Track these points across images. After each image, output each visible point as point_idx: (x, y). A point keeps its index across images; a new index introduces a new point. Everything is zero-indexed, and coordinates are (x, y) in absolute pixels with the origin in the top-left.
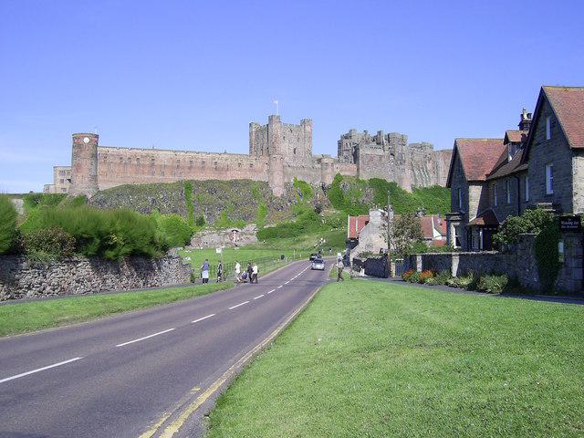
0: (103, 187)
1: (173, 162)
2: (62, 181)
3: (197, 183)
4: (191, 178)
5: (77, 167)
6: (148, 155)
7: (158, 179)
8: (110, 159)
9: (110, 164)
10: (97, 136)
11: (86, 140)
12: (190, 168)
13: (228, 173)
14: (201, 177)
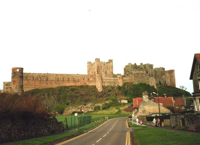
0: (26, 89)
2: (7, 88)
4: (63, 85)
5: (14, 82)
7: (49, 86)
10: (22, 69)
11: (18, 70)
14: (67, 84)
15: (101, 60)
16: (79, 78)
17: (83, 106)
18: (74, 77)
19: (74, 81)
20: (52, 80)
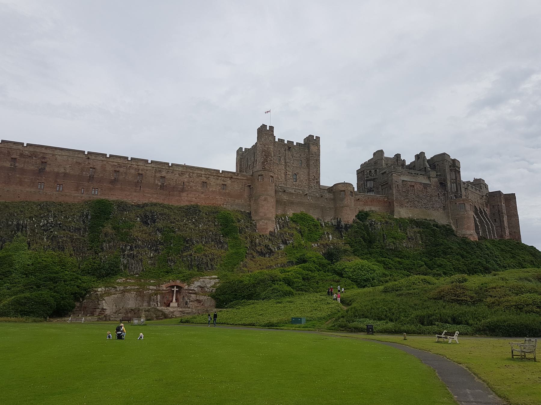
3: (123, 206)
6: (33, 155)
12: (114, 182)
13: (184, 194)
14: (133, 197)
15: (278, 135)
17: (178, 283)
18: (164, 174)
19: (162, 187)
20: (66, 175)
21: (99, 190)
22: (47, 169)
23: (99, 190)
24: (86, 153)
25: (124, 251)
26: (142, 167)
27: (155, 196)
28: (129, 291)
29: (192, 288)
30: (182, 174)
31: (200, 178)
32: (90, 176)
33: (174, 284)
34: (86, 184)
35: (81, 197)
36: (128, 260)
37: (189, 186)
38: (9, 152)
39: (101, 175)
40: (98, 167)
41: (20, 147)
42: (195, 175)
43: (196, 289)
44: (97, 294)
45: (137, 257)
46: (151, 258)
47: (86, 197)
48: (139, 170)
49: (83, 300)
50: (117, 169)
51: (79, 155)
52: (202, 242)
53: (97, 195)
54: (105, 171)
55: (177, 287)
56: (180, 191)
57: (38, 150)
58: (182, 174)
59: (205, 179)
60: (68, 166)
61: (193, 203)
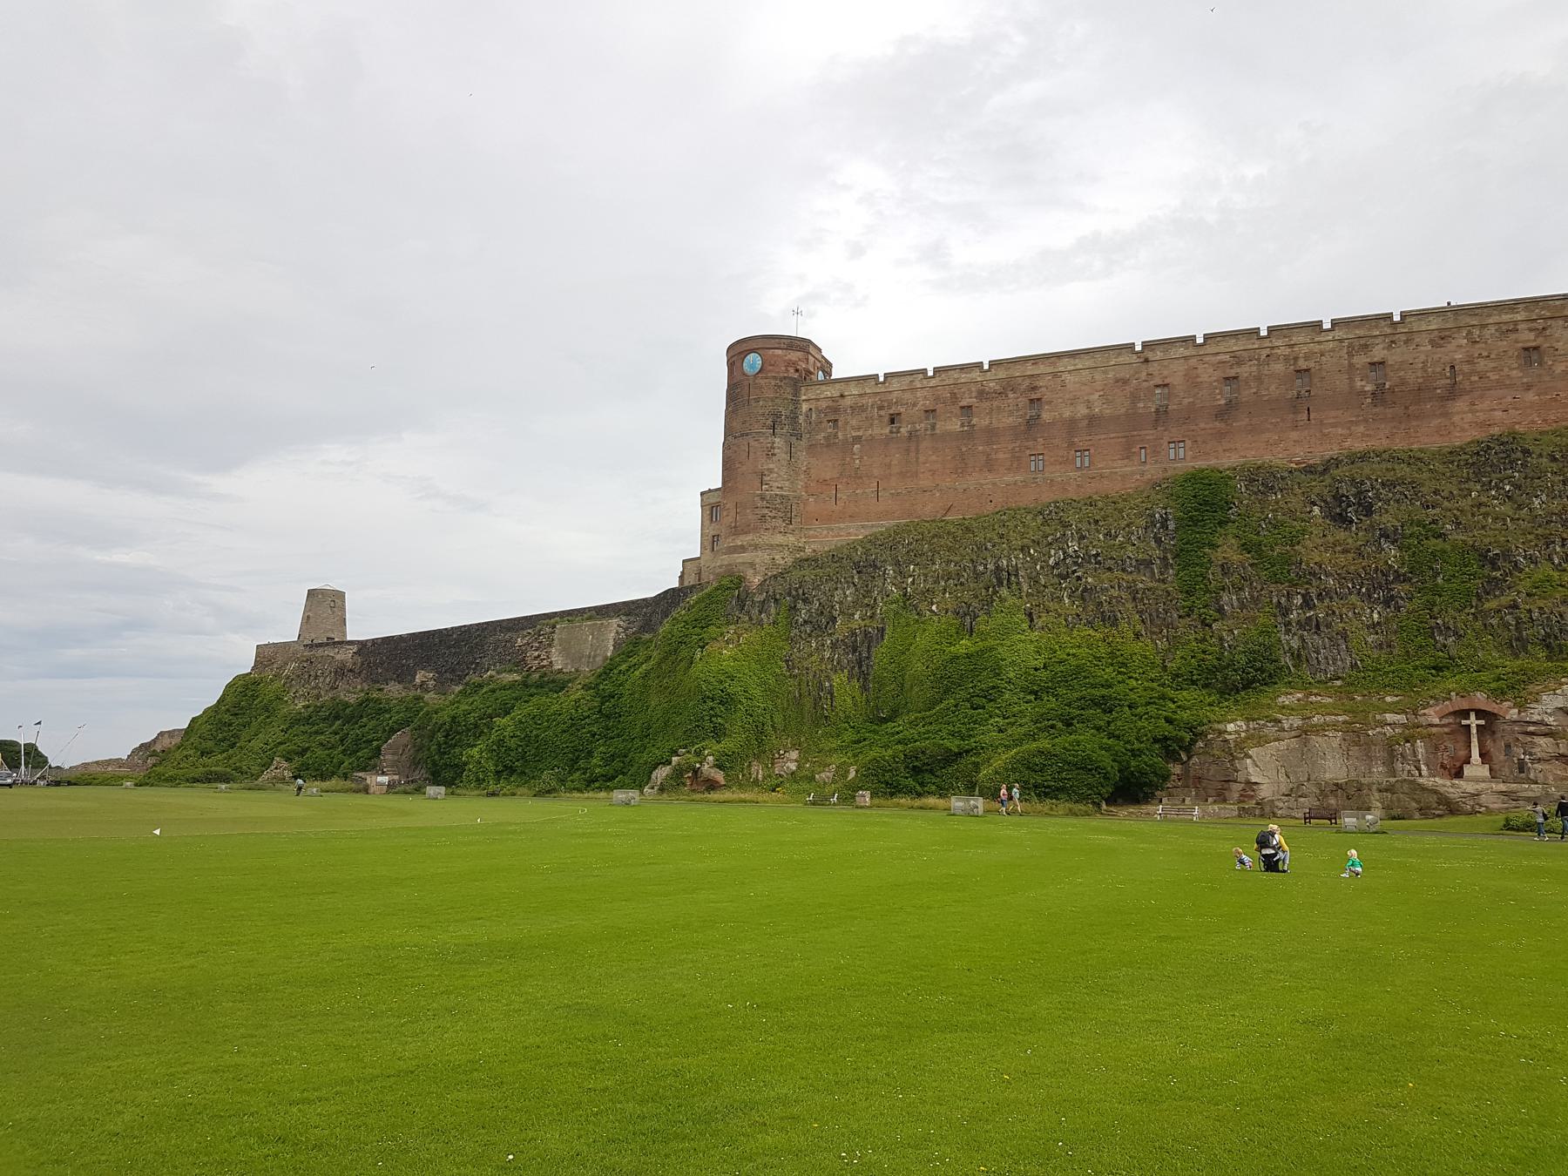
1: (1135, 398)
3: (1263, 480)
6: (1008, 386)
8: (851, 426)
9: (847, 446)
12: (1225, 413)
13: (1461, 405)
14: (1288, 448)
16: (1457, 350)
17: (1481, 699)
18: (1378, 353)
19: (1379, 396)
20: (1093, 421)
21: (1189, 443)
22: (1046, 416)
23: (1189, 443)
24: (1138, 348)
25: (1286, 612)
26: (1305, 349)
27: (1361, 429)
28: (1320, 730)
29: (1536, 718)
30: (1442, 338)
31: (1513, 336)
32: (1157, 411)
33: (1464, 705)
34: (1150, 434)
35: (1142, 475)
36: (1302, 639)
37: (1473, 372)
38: (953, 395)
39: (1186, 401)
40: (1177, 380)
41: (976, 375)
42: (1492, 329)
43: (1550, 720)
44: (1226, 741)
45: (1329, 626)
46: (1374, 625)
47: (1153, 471)
48: (1296, 359)
49: (1189, 758)
50: (1232, 373)
51: (1121, 359)
52: (1550, 559)
53: (1183, 459)
54: (1197, 385)
55: (1480, 714)
56: (1442, 398)
57: (1017, 372)
58: (1442, 338)
59: (1532, 336)
60: (1096, 396)
61: (1496, 431)
